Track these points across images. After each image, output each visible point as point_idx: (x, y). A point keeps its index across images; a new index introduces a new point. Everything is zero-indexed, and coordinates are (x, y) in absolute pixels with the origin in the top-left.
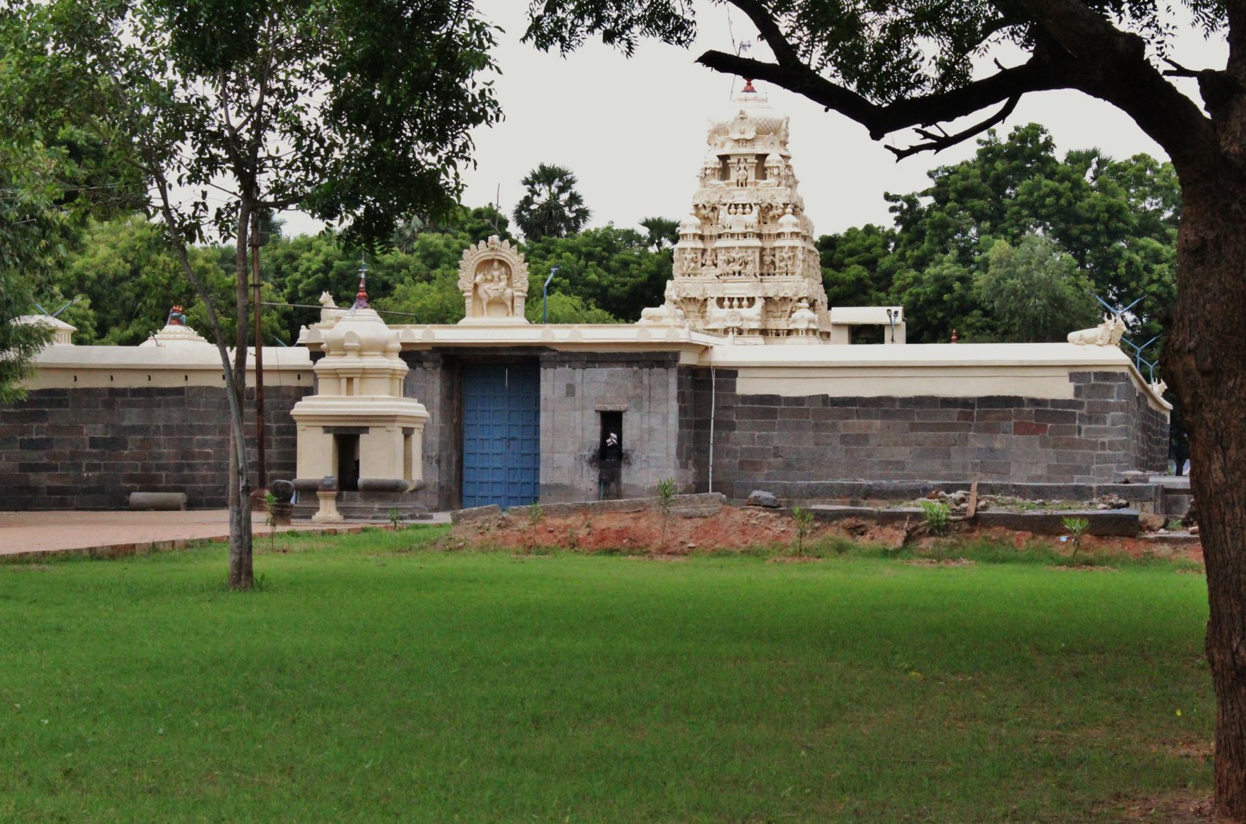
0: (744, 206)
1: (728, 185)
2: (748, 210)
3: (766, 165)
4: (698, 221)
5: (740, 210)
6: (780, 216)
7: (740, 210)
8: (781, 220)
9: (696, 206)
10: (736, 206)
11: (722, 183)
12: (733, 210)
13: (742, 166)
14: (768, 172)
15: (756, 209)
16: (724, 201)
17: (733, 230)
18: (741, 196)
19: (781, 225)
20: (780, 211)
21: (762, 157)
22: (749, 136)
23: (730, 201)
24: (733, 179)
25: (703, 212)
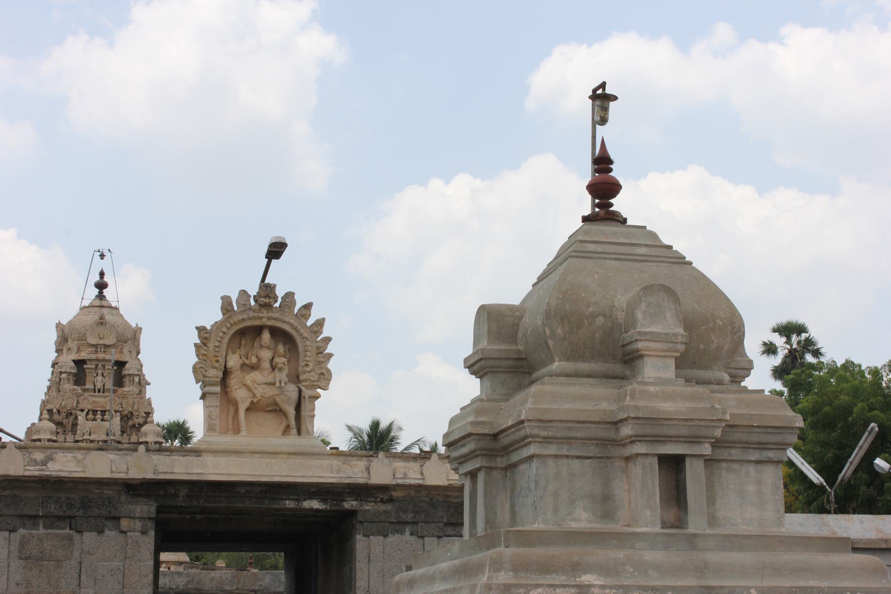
0: (103, 412)
1: (84, 390)
2: (107, 417)
3: (125, 372)
4: (53, 426)
5: (99, 416)
6: (141, 425)
7: (99, 416)
8: (144, 428)
9: (50, 411)
10: (95, 412)
11: (79, 389)
12: (91, 416)
13: (100, 372)
14: (126, 380)
15: (117, 419)
16: (81, 407)
17: (92, 437)
18: (101, 401)
19: (146, 435)
20: (141, 420)
21: (121, 364)
22: (111, 341)
23: (90, 407)
24: (89, 386)
25: (56, 417)
